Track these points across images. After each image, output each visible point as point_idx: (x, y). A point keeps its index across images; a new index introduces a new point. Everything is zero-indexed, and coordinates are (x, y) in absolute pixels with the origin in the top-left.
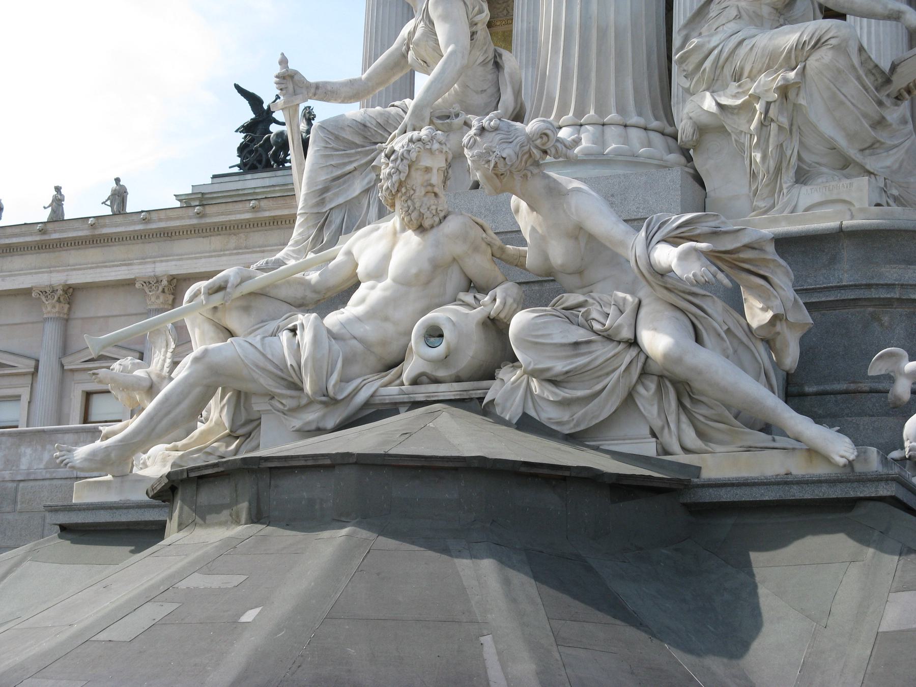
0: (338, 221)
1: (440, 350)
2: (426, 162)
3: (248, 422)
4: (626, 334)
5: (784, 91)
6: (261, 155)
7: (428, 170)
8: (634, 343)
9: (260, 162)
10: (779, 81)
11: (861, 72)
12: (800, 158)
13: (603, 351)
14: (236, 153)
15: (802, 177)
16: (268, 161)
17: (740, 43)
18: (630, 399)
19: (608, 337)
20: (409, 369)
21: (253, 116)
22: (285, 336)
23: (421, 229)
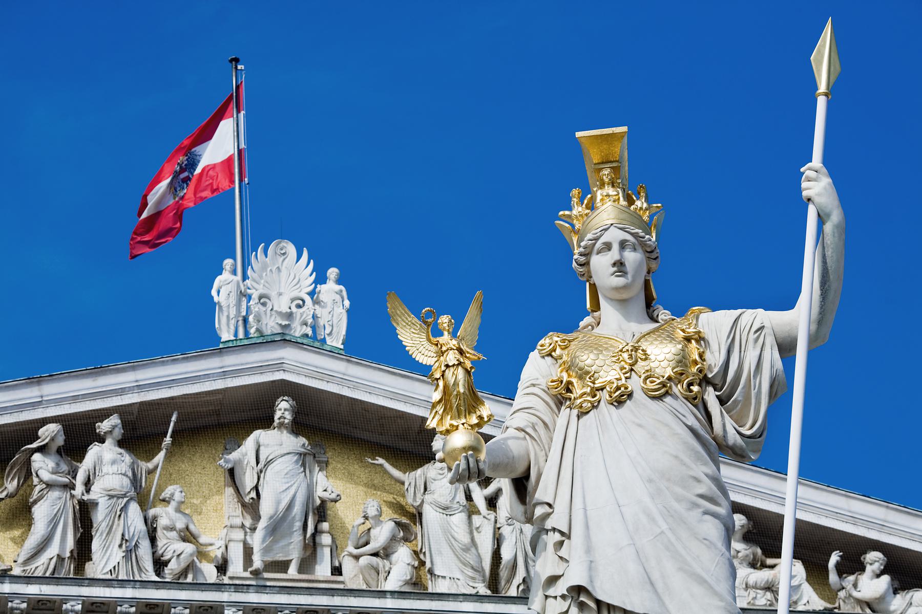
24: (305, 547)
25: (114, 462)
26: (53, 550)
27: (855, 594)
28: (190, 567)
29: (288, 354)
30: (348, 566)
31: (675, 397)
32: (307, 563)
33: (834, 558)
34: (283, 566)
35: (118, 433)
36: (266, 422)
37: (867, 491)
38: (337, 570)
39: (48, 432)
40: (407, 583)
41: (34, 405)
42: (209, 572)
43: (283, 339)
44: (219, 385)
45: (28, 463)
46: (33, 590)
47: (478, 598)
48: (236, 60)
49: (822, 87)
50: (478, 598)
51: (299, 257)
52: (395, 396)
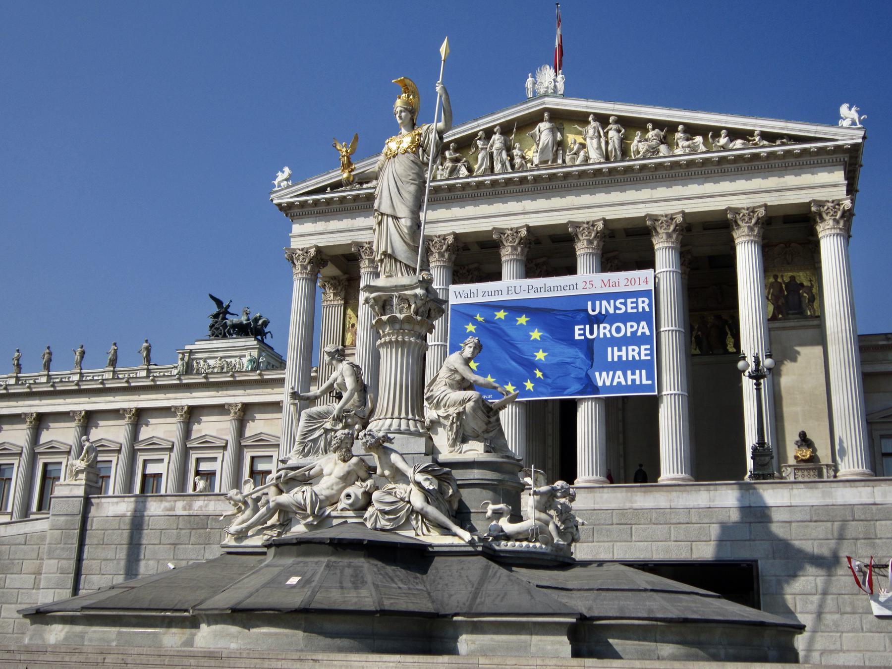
0: (310, 445)
1: (350, 501)
2: (347, 441)
3: (288, 520)
4: (407, 499)
5: (459, 414)
6: (221, 330)
7: (347, 443)
8: (409, 502)
9: (221, 334)
10: (457, 411)
11: (483, 408)
12: (463, 434)
13: (401, 504)
14: (208, 328)
15: (464, 440)
16: (225, 333)
17: (446, 395)
18: (408, 519)
19: (402, 499)
20: (340, 506)
21: (218, 310)
22: (301, 494)
23: (344, 461)
24: (554, 155)
25: (498, 140)
26: (483, 168)
27: (718, 144)
28: (522, 165)
29: (547, 99)
30: (567, 159)
31: (409, 153)
32: (555, 160)
33: (710, 134)
34: (546, 162)
35: (499, 131)
36: (542, 121)
37: (720, 111)
38: (564, 161)
39: (480, 133)
40: (583, 161)
41: (476, 127)
42: (529, 165)
43: (546, 95)
44: (527, 112)
45: (476, 143)
46: (476, 179)
47: (600, 163)
48: (558, 4)
49: (443, 59)
50: (600, 163)
51: (550, 68)
52: (577, 106)
